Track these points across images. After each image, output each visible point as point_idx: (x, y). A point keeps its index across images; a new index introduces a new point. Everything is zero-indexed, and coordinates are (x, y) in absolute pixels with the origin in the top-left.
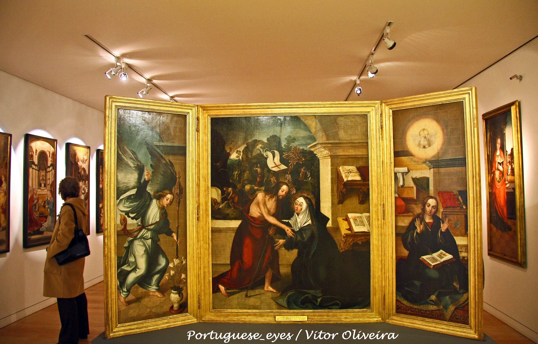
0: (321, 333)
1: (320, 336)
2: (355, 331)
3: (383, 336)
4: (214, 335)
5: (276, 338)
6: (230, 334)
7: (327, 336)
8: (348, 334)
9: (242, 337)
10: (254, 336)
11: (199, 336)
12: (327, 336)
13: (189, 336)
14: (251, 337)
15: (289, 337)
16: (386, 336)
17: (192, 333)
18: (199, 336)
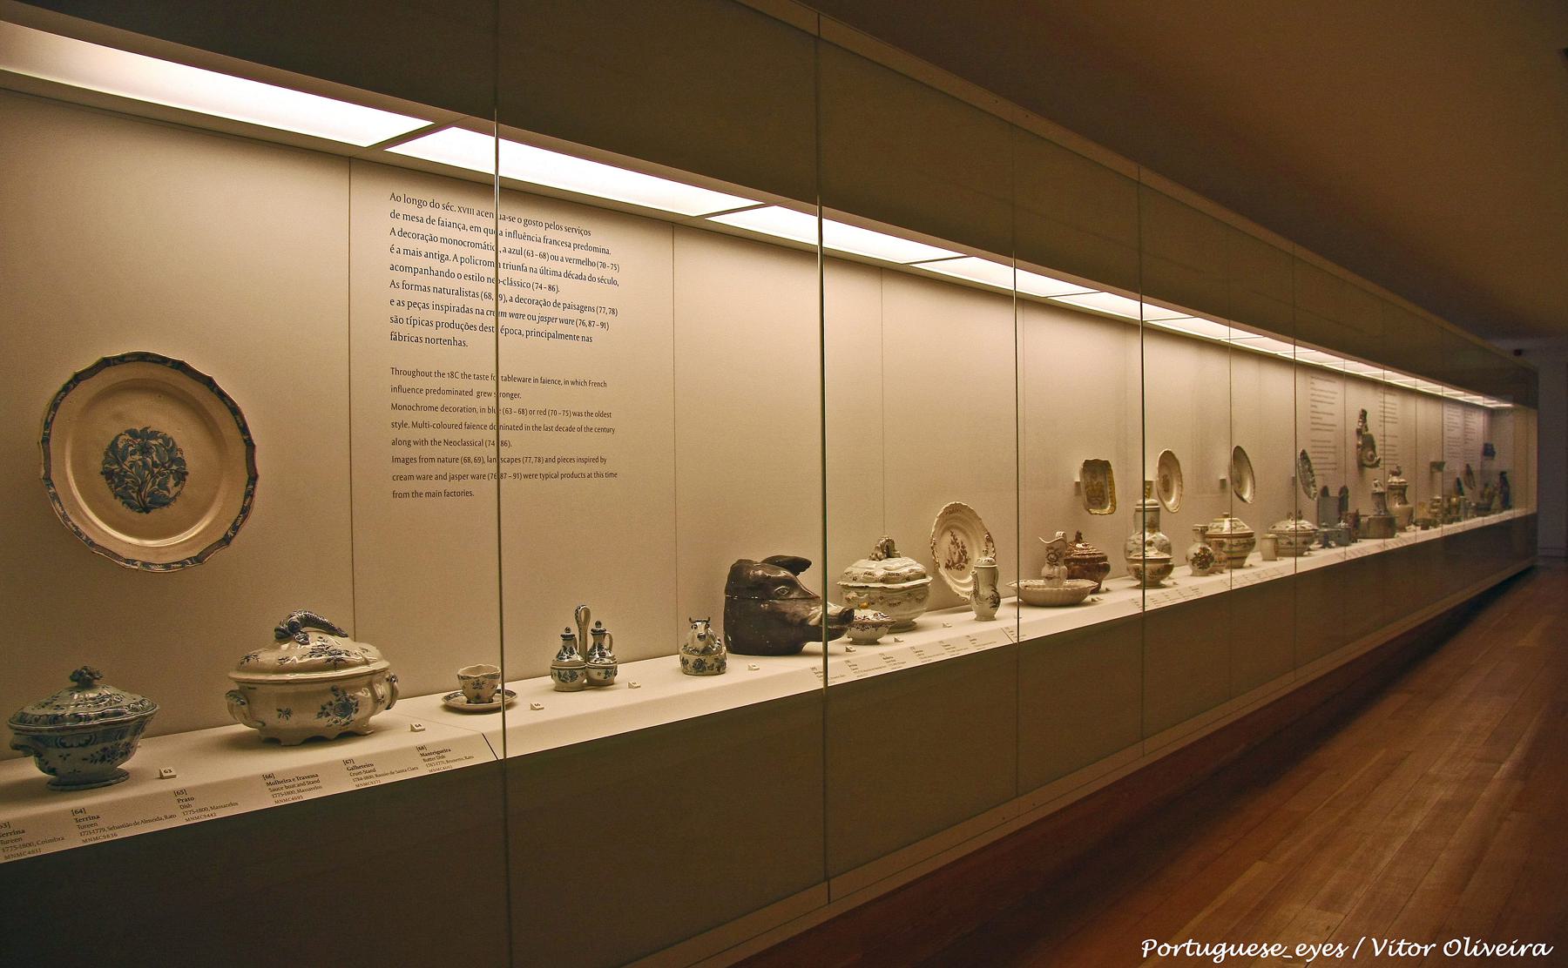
0: (1402, 943)
1: (1400, 950)
3: (1523, 950)
4: (1193, 948)
7: (1414, 950)
8: (1455, 945)
9: (1248, 951)
10: (1272, 949)
11: (1164, 950)
12: (1414, 950)
13: (1146, 949)
15: (1341, 951)
16: (1529, 951)
17: (1151, 944)
18: (1164, 950)
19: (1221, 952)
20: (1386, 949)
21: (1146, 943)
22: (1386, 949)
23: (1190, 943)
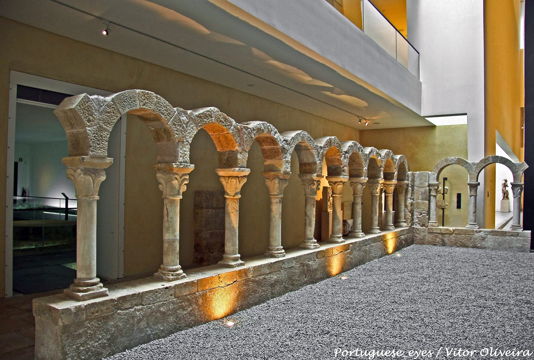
0: (460, 350)
1: (459, 353)
2: (492, 348)
4: (359, 353)
5: (418, 355)
6: (374, 351)
9: (386, 354)
10: (397, 353)
11: (345, 353)
14: (394, 354)
18: (345, 353)
19: (373, 354)
20: (452, 352)
21: (336, 350)
22: (452, 352)
23: (357, 350)
